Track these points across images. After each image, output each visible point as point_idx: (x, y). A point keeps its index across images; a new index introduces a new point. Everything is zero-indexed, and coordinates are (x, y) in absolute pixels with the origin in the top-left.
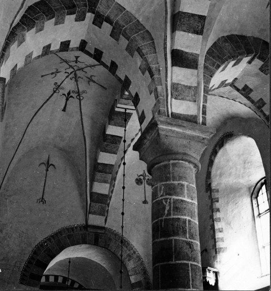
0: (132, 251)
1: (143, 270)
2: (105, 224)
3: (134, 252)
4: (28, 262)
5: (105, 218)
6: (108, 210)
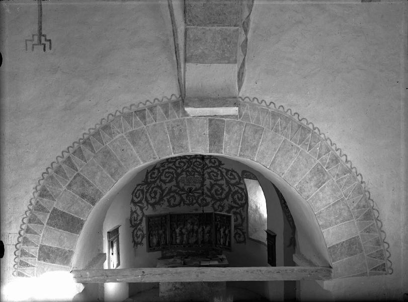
0: (327, 158)
1: (364, 207)
2: (240, 88)
3: (336, 160)
4: (30, 221)
5: (236, 68)
6: (246, 40)
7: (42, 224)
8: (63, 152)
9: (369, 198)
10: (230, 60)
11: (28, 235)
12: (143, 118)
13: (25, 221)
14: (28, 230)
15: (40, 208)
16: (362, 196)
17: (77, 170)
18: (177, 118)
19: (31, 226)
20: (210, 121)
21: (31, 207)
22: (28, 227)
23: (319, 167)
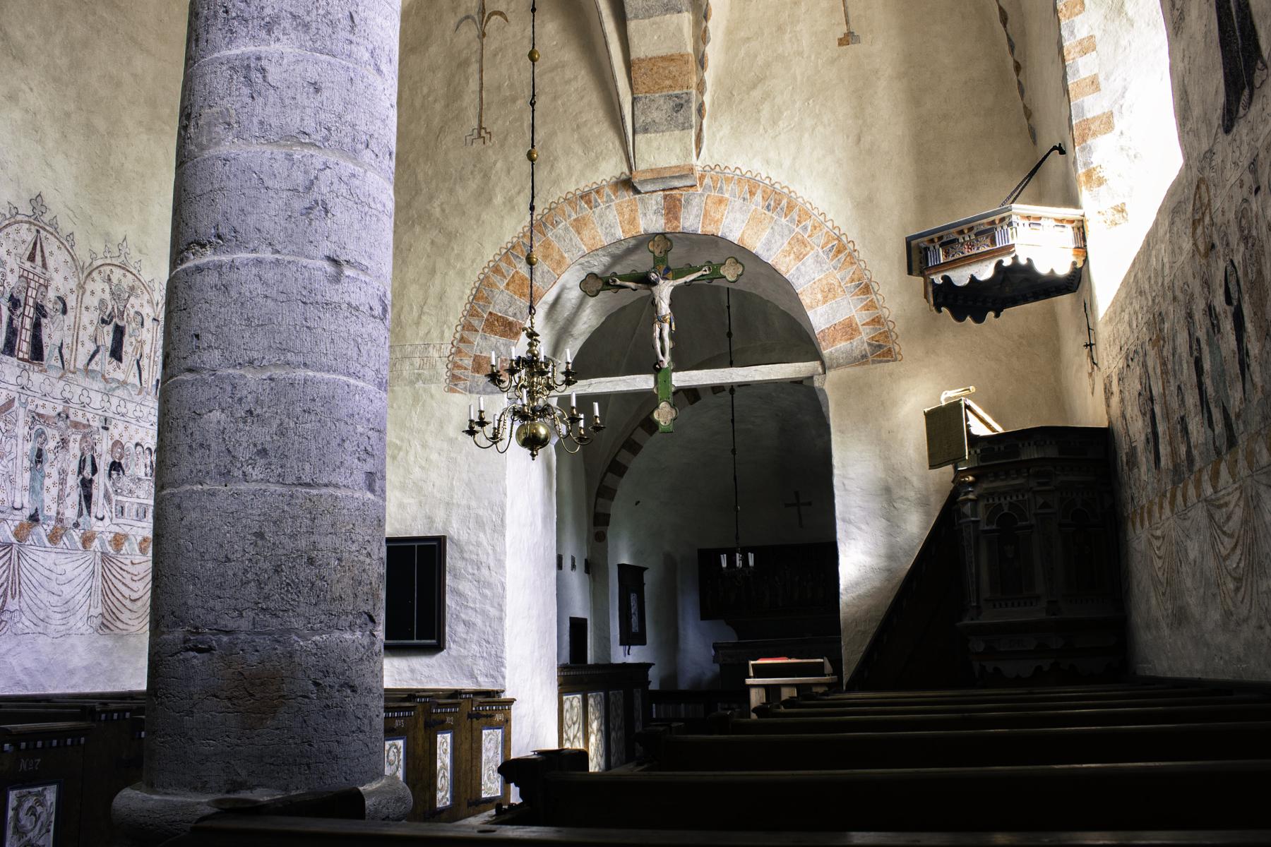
2: (698, 155)
5: (693, 133)
7: (476, 331)
8: (501, 248)
9: (865, 269)
10: (685, 126)
11: (461, 345)
12: (588, 202)
13: (459, 328)
14: (462, 340)
15: (473, 313)
16: (855, 266)
17: (515, 268)
18: (627, 198)
19: (466, 334)
20: (665, 197)
21: (465, 313)
22: (461, 335)
23: (799, 236)
